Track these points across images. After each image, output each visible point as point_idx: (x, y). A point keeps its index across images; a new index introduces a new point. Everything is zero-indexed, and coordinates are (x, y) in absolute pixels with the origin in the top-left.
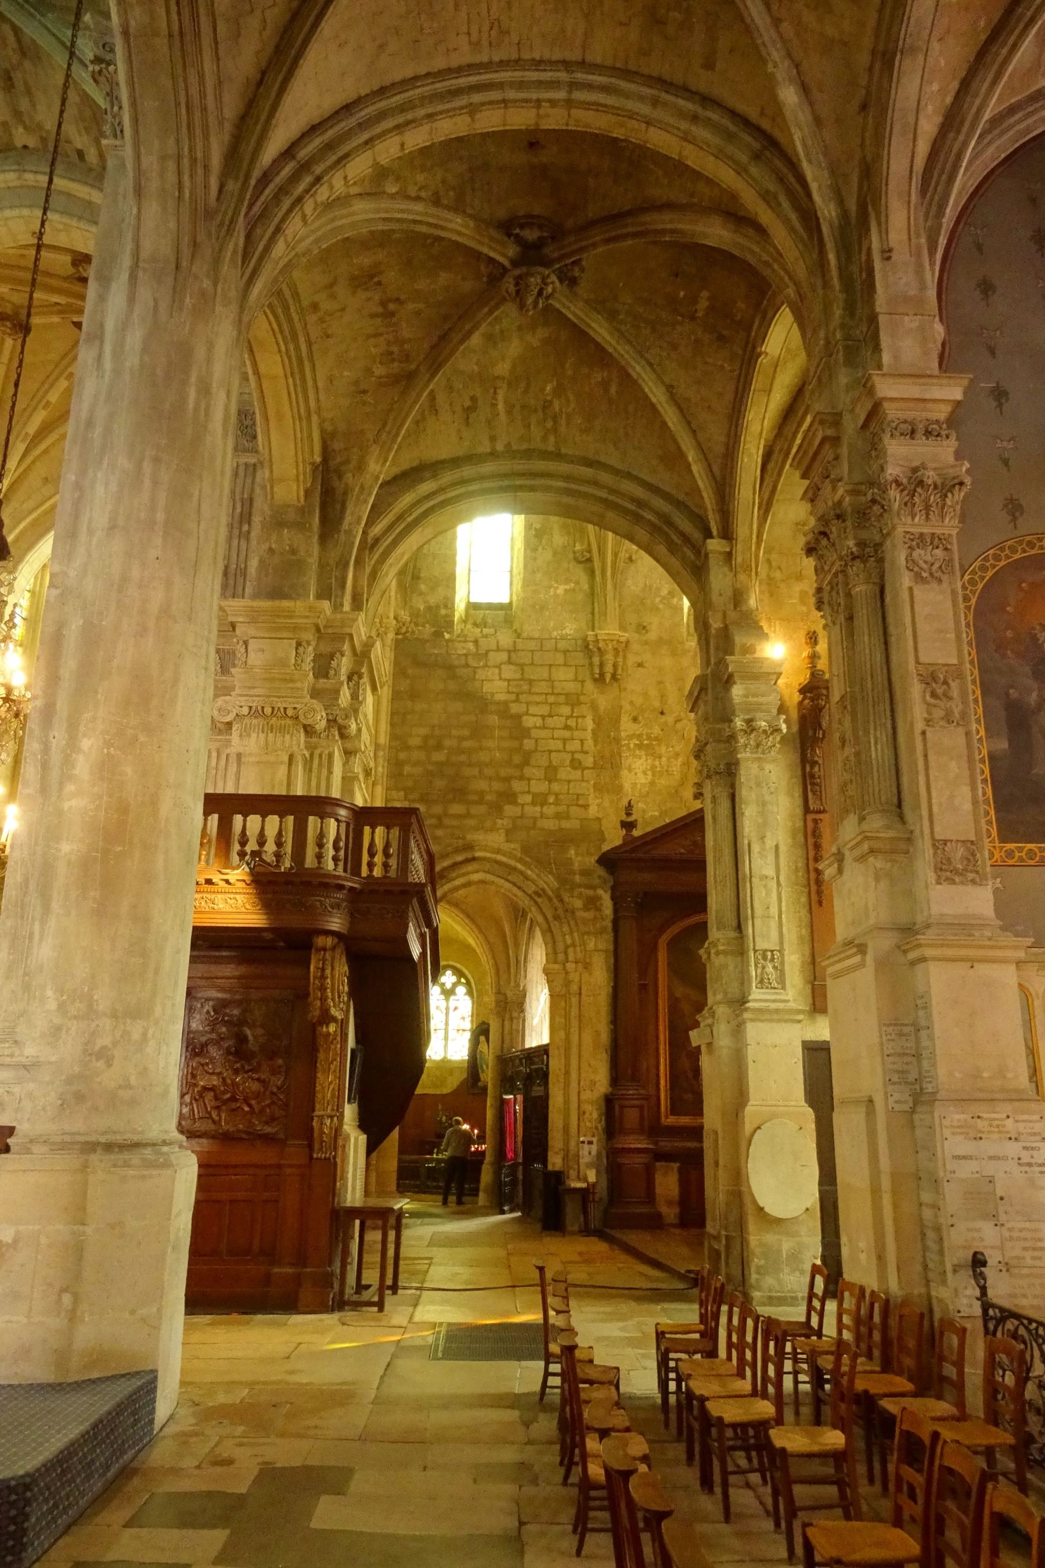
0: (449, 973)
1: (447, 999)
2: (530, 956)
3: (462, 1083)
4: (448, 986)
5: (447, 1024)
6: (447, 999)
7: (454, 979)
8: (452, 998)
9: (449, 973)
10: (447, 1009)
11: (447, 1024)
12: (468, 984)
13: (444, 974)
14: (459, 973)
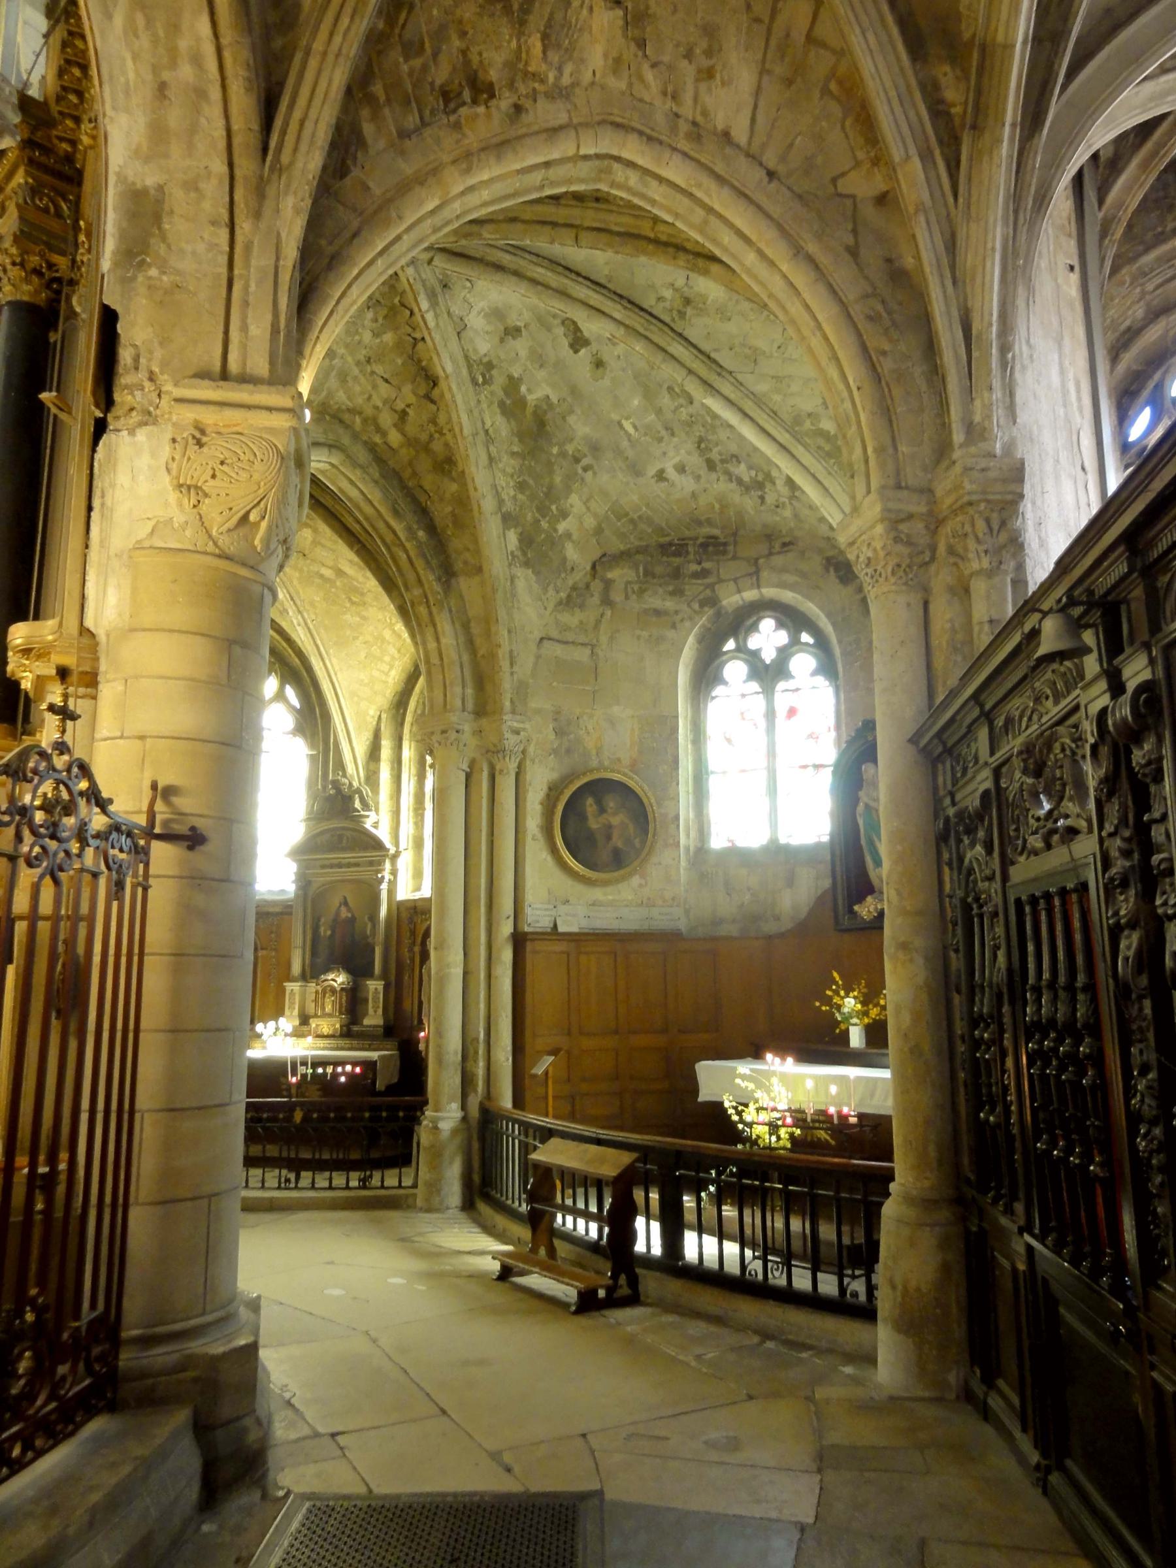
0: (767, 624)
1: (768, 691)
2: (1020, 348)
3: (820, 901)
4: (769, 656)
5: (771, 753)
6: (768, 691)
7: (782, 637)
8: (781, 685)
9: (767, 624)
10: (770, 715)
11: (771, 753)
12: (822, 645)
13: (754, 628)
14: (792, 619)
